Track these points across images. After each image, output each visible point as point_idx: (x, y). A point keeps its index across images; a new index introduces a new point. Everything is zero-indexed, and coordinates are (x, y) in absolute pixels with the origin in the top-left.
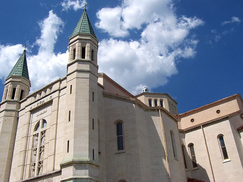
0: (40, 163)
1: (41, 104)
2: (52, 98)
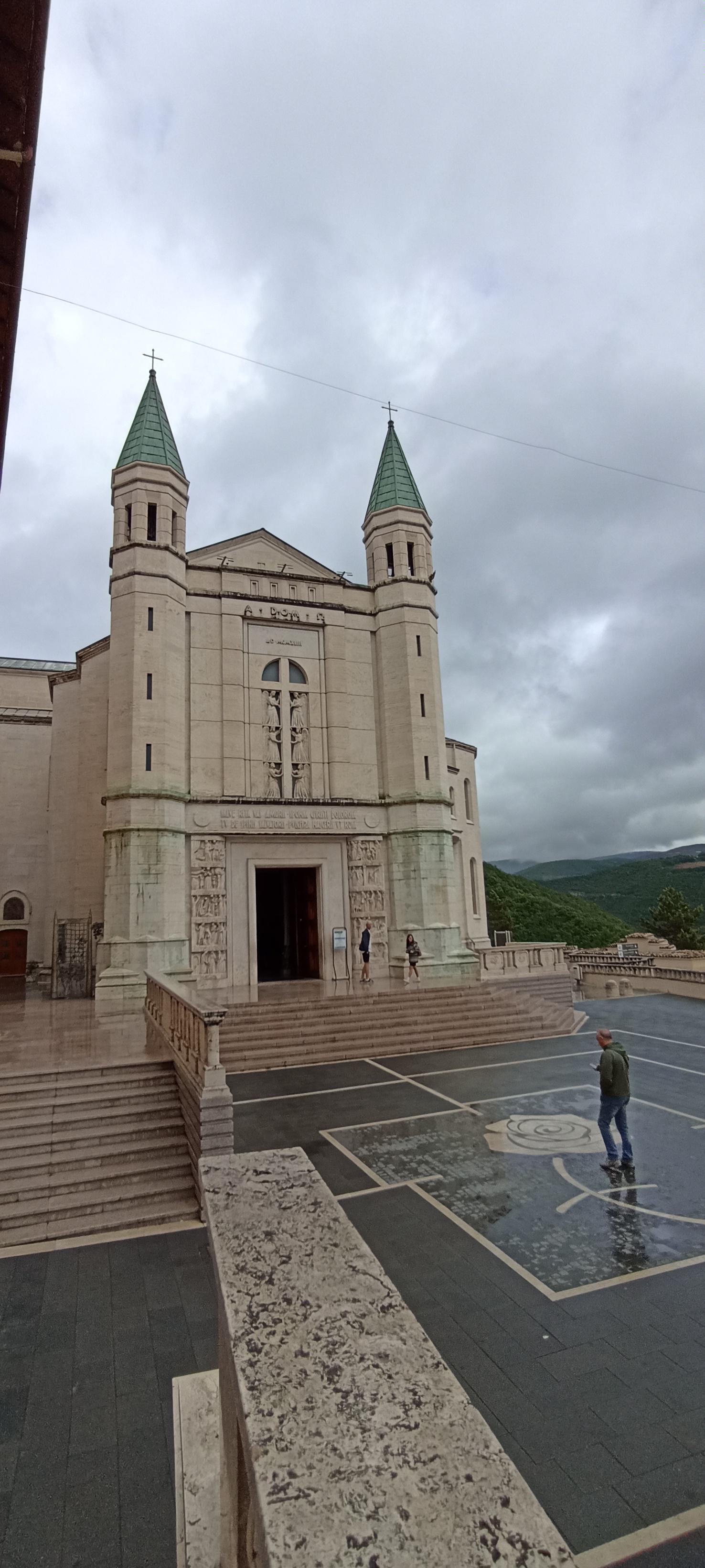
0: (295, 766)
1: (289, 618)
2: (327, 623)
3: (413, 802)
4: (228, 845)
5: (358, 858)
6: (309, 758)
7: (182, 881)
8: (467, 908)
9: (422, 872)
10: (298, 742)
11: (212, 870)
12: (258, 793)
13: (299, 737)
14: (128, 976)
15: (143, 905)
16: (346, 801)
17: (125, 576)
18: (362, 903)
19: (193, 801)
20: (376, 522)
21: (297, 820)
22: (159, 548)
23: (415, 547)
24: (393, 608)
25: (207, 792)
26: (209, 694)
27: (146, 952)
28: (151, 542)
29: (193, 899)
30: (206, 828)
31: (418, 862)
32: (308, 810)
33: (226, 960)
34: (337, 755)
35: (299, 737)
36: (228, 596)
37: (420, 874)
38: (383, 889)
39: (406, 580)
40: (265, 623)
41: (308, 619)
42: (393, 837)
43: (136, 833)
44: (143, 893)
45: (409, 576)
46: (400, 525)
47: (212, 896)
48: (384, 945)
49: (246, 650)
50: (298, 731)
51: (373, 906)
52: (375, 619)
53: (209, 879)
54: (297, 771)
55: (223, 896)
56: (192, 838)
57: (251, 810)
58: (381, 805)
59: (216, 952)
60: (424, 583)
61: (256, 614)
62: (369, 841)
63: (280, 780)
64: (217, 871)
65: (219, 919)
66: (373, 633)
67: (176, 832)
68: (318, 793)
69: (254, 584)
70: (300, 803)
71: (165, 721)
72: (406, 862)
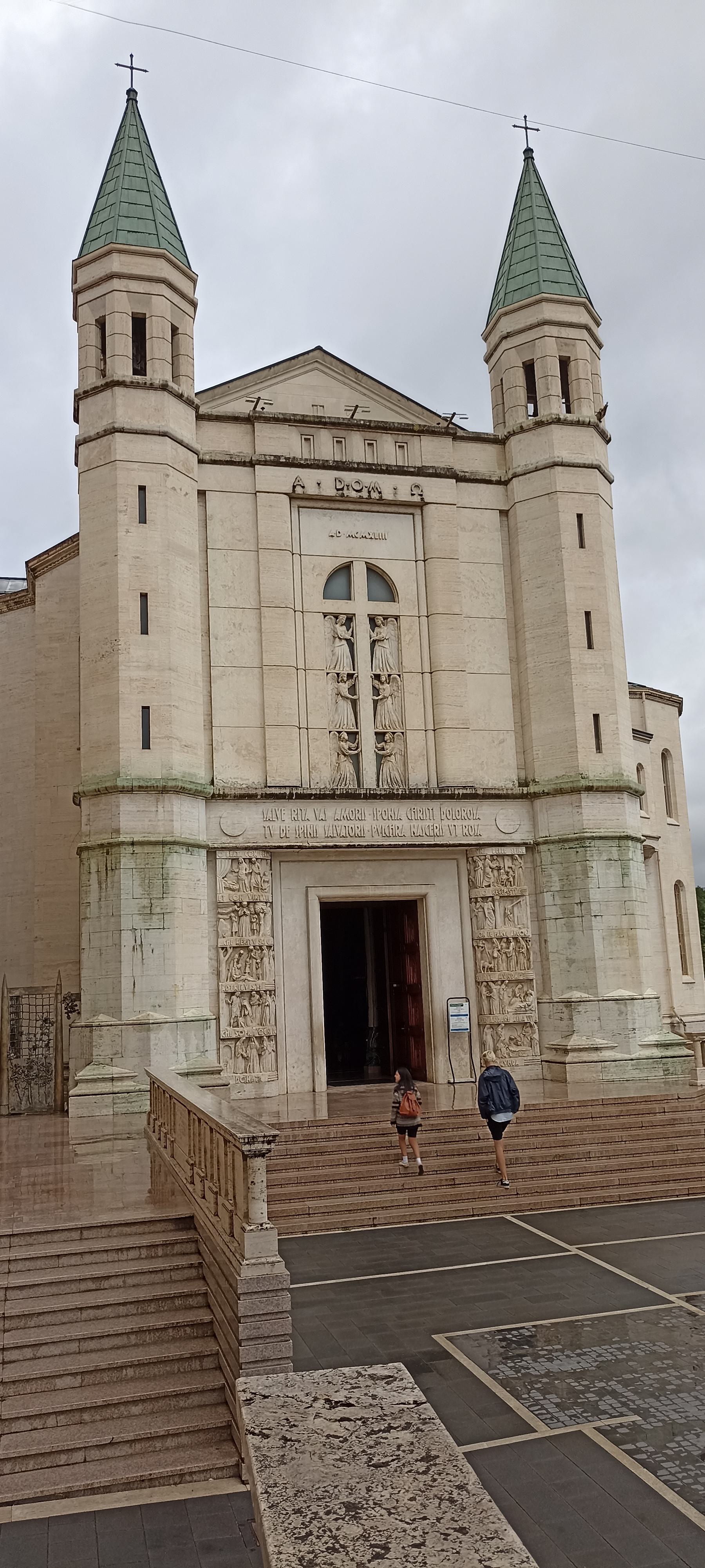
0: (380, 736)
1: (365, 494)
3: (576, 791)
4: (276, 865)
5: (485, 884)
6: (403, 723)
7: (204, 924)
8: (671, 965)
9: (595, 908)
10: (385, 697)
11: (251, 906)
12: (322, 779)
13: (386, 689)
14: (121, 1079)
15: (143, 964)
16: (465, 791)
17: (99, 436)
18: (494, 958)
19: (219, 795)
20: (506, 325)
21: (385, 824)
22: (151, 387)
23: (572, 364)
24: (537, 469)
25: (240, 782)
26: (240, 625)
27: (149, 1039)
28: (138, 378)
29: (221, 952)
30: (240, 838)
31: (586, 889)
32: (402, 809)
33: (276, 1052)
34: (448, 716)
35: (386, 689)
36: (266, 463)
37: (589, 911)
38: (529, 934)
39: (558, 421)
40: (326, 505)
41: (395, 494)
42: (543, 848)
43: (130, 849)
44: (141, 945)
45: (563, 414)
46: (546, 327)
47: (252, 947)
48: (531, 1026)
49: (296, 550)
50: (383, 679)
51: (513, 963)
52: (506, 490)
53: (246, 920)
54: (383, 744)
55: (269, 947)
56: (219, 854)
57: (311, 809)
58: (522, 796)
59: (260, 1038)
60: (589, 425)
61: (312, 490)
62: (503, 856)
63: (356, 760)
64: (259, 906)
65: (263, 984)
66: (504, 513)
67: (191, 846)
68: (418, 778)
69: (307, 440)
70: (390, 796)
71: (170, 669)
72: (565, 891)
